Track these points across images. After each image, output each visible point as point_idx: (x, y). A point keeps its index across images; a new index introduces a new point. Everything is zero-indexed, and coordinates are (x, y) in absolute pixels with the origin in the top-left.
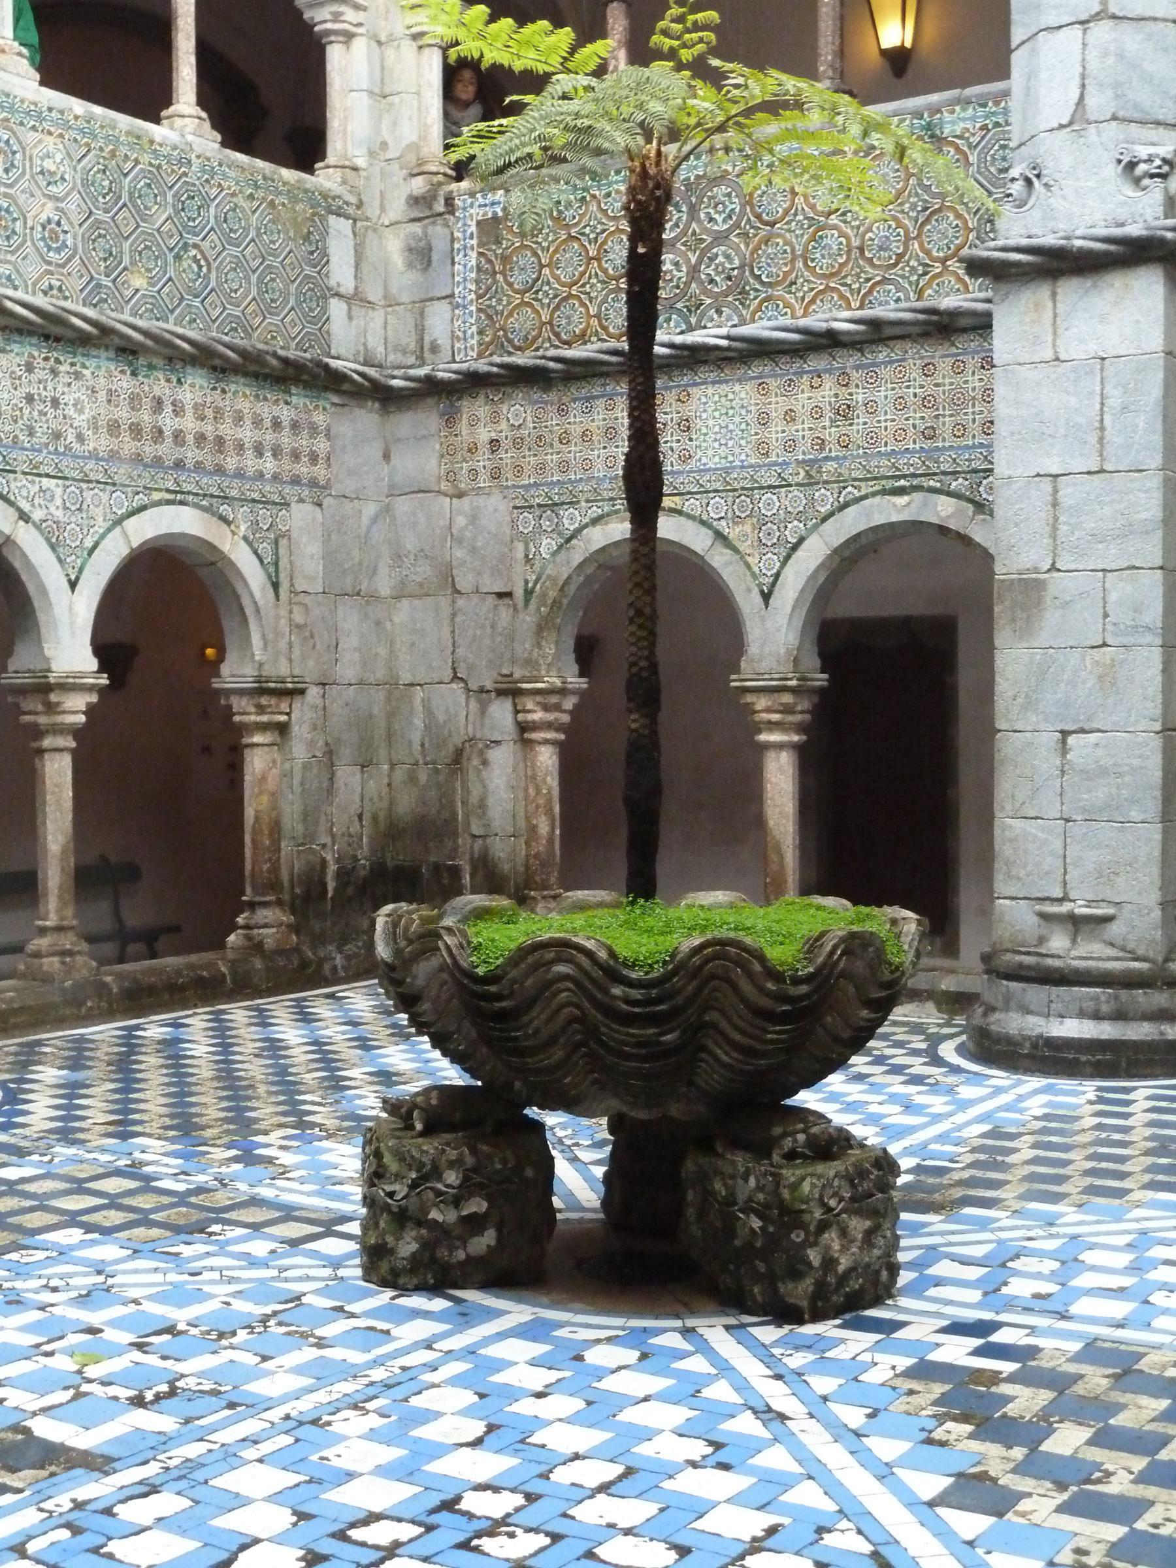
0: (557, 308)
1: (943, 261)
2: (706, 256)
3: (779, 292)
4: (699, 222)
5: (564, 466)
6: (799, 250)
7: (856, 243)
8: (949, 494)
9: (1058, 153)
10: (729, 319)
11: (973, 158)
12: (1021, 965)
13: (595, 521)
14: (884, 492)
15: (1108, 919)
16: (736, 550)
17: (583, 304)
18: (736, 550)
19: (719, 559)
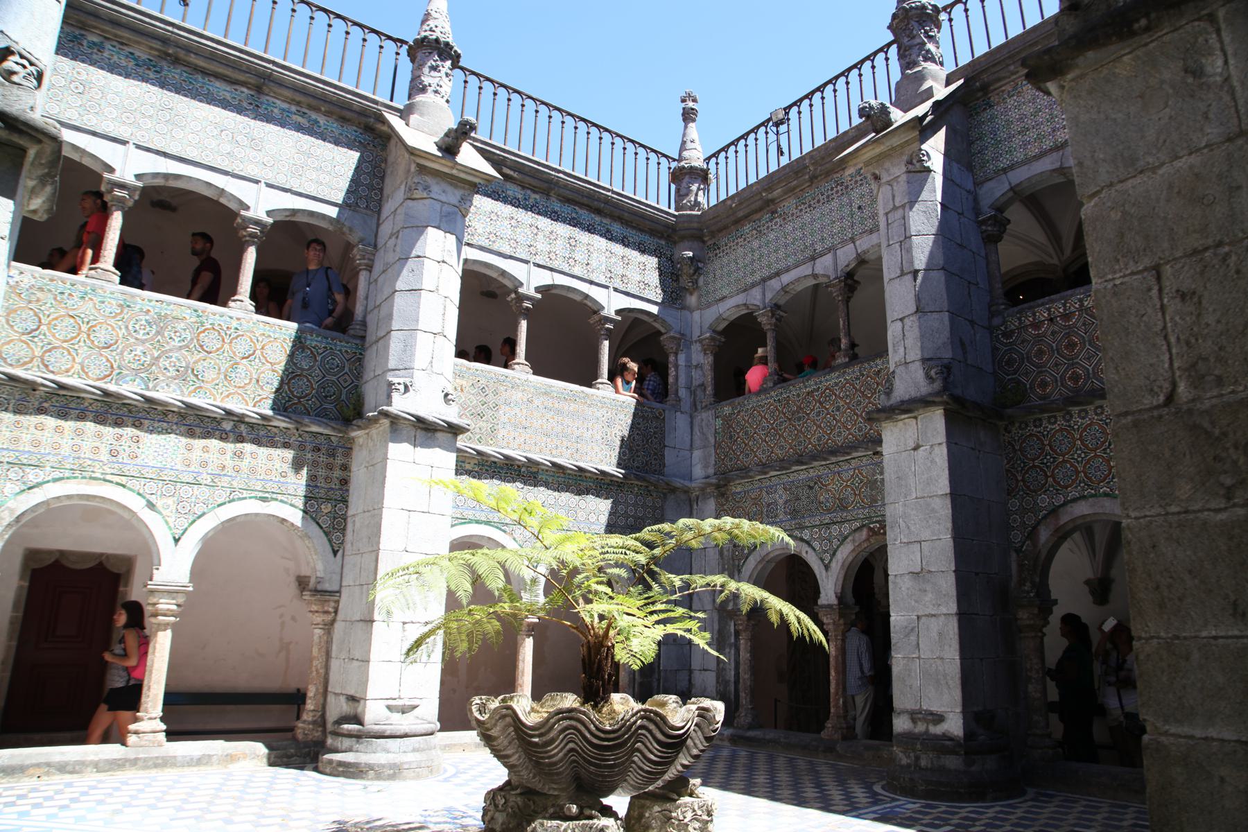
0: (50, 351)
1: (299, 398)
2: (165, 354)
3: (208, 386)
4: (163, 336)
5: (36, 444)
6: (223, 370)
7: (255, 376)
8: (292, 505)
9: (419, 379)
10: (174, 391)
11: (319, 358)
12: (384, 731)
13: (55, 480)
14: (256, 498)
15: (416, 707)
16: (160, 513)
17: (69, 353)
18: (160, 513)
19: (147, 516)
